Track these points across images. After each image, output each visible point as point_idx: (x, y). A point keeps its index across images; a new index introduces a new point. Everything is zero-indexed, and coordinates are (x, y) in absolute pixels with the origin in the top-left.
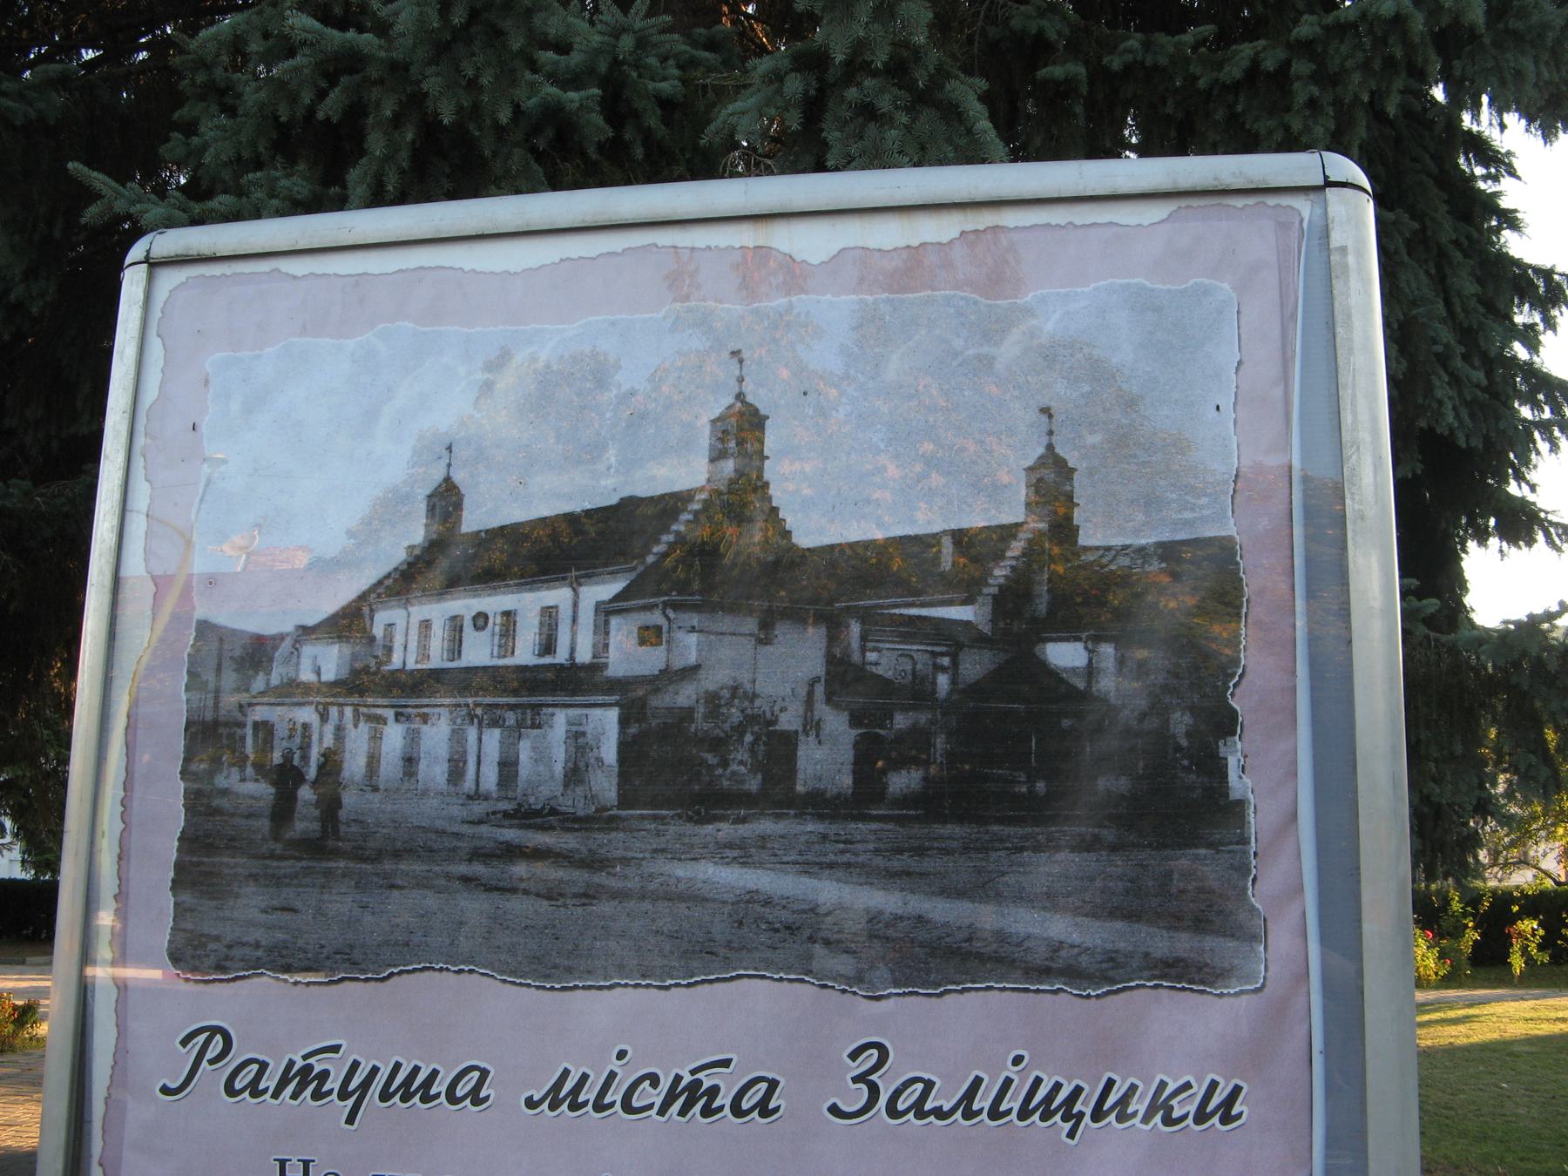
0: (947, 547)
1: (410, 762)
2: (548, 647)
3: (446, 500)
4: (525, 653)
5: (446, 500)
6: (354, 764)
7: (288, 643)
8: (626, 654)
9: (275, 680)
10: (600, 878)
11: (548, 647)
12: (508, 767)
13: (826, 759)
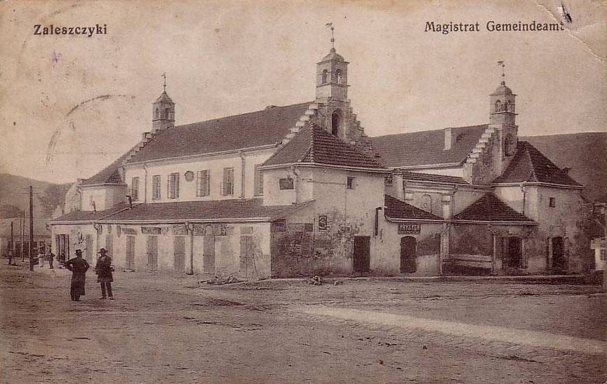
0: (448, 135)
1: (152, 255)
2: (229, 189)
3: (165, 108)
4: (216, 195)
5: (165, 108)
6: (118, 260)
7: (74, 187)
8: (274, 197)
9: (67, 211)
10: (264, 315)
11: (229, 189)
12: (209, 257)
13: (386, 251)
